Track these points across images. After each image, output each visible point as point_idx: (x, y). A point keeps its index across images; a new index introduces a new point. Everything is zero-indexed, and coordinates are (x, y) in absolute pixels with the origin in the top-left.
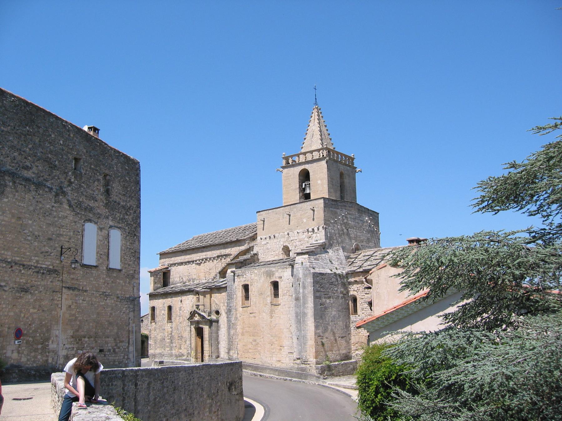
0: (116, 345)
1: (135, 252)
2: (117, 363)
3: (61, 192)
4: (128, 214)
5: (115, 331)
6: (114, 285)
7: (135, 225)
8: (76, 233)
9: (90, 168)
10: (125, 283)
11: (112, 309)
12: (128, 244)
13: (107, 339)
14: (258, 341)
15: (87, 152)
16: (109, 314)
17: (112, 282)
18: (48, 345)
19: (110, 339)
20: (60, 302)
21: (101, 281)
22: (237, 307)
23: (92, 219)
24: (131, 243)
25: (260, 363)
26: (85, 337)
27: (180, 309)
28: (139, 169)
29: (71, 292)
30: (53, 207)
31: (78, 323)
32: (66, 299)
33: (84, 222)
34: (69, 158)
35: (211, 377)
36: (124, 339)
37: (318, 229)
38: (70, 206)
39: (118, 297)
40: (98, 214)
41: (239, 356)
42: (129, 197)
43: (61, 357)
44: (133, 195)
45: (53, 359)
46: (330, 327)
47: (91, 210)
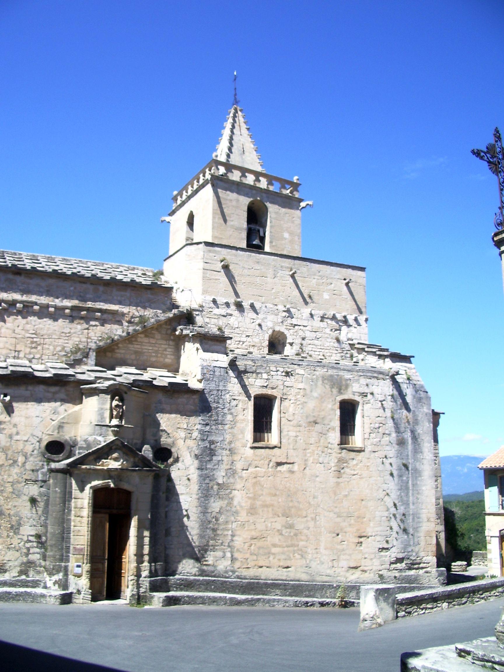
22: (237, 445)
25: (304, 577)
41: (237, 565)
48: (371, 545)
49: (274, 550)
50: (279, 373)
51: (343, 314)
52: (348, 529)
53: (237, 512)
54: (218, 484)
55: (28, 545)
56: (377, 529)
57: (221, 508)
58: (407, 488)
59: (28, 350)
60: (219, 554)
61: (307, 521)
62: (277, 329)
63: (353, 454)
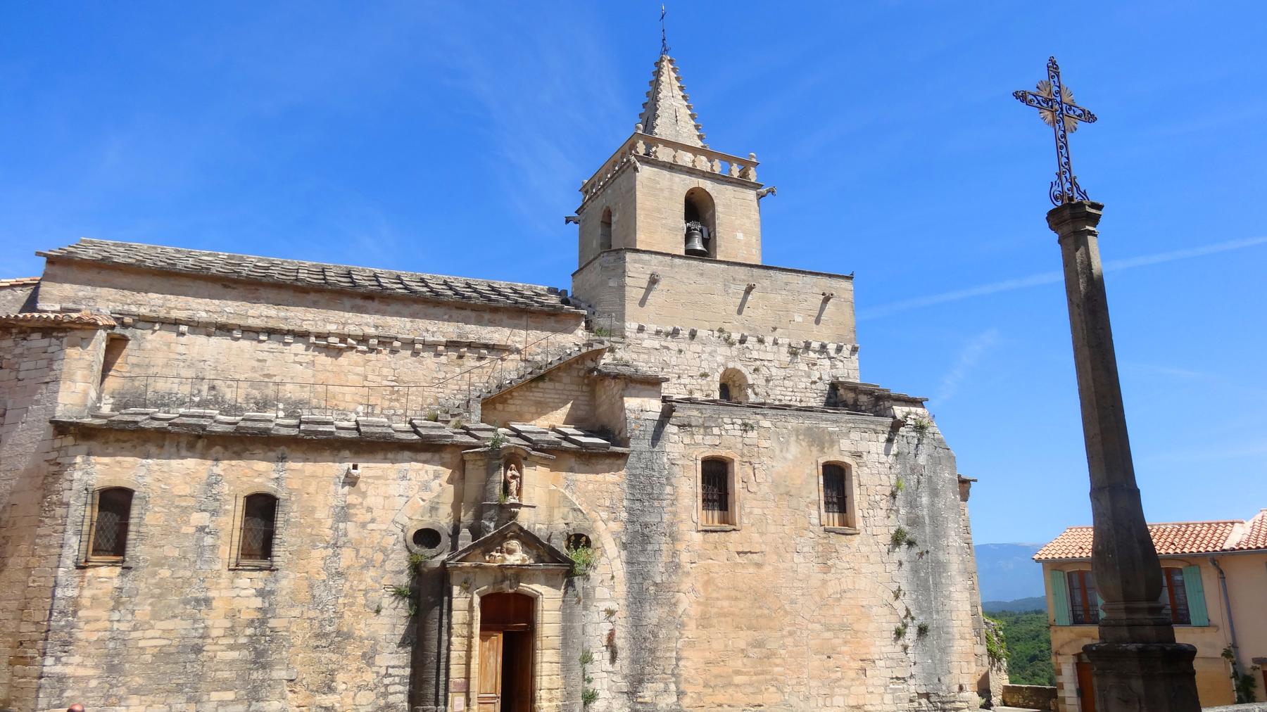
14: (772, 645)
37: (839, 350)
41: (686, 701)
49: (738, 679)
50: (737, 427)
53: (683, 625)
54: (656, 584)
55: (386, 681)
56: (884, 649)
57: (660, 618)
58: (927, 589)
59: (386, 404)
61: (783, 637)
62: (731, 365)
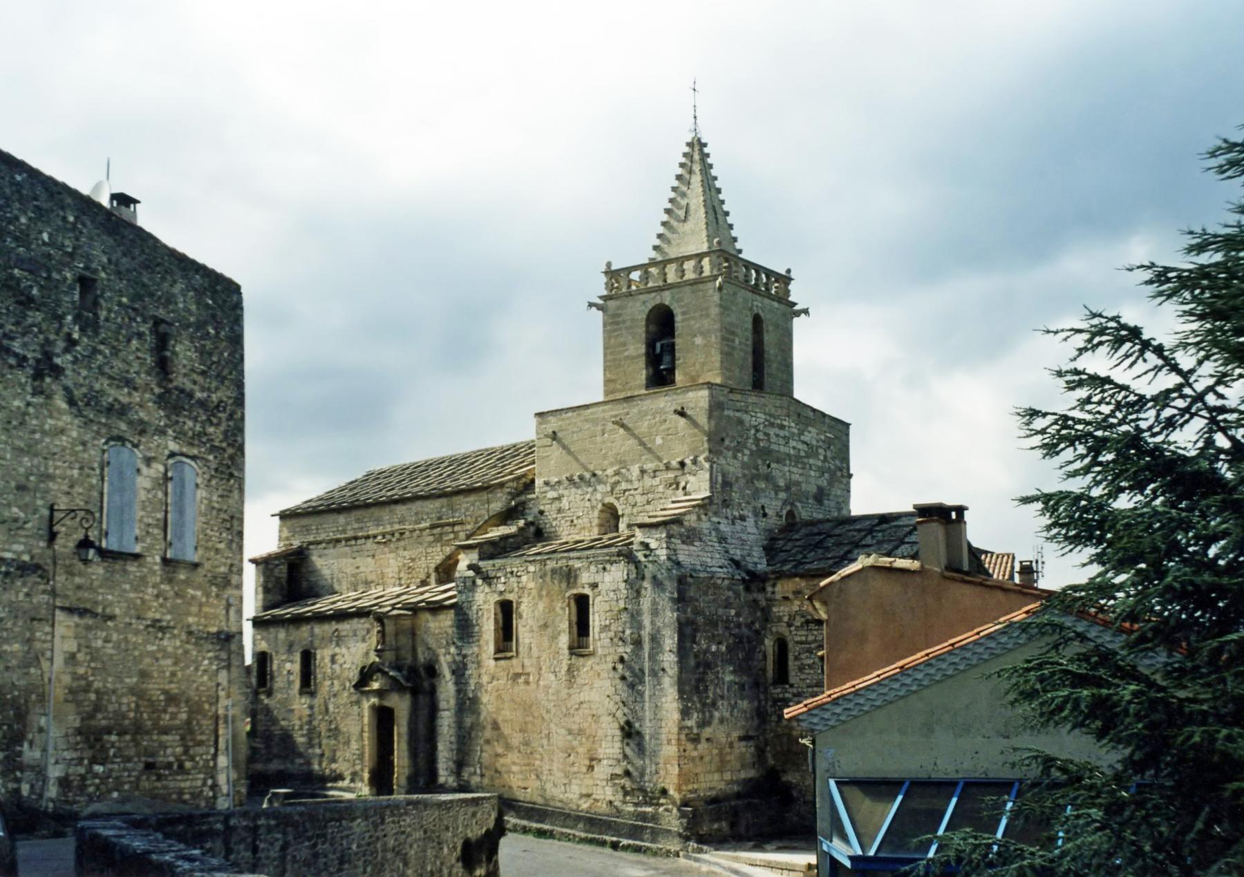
0: (186, 752)
1: (232, 517)
2: (187, 797)
3: (45, 368)
4: (215, 421)
5: (184, 716)
6: (179, 601)
7: (230, 451)
8: (87, 470)
9: (120, 304)
10: (208, 595)
11: (175, 664)
12: (215, 498)
13: (164, 738)
15: (110, 261)
16: (168, 674)
17: (177, 595)
18: (20, 754)
19: (169, 738)
20: (48, 645)
21: (150, 590)
22: (484, 656)
23: (127, 436)
24: (221, 496)
25: (540, 800)
26: (110, 733)
27: (333, 661)
28: (238, 306)
29: (76, 619)
30: (28, 404)
31: (93, 696)
32: (63, 637)
33: (106, 443)
34: (65, 279)
35: (425, 832)
36: (204, 738)
38: (71, 402)
39: (190, 633)
40: (141, 422)
42: (218, 376)
43: (52, 782)
44: (225, 372)
45: (32, 786)
46: (717, 714)
47: (121, 411)
48: (603, 770)
49: (514, 768)
51: (679, 459)
52: (581, 750)
53: (484, 728)
60: (472, 769)
62: (607, 500)
63: (581, 660)
